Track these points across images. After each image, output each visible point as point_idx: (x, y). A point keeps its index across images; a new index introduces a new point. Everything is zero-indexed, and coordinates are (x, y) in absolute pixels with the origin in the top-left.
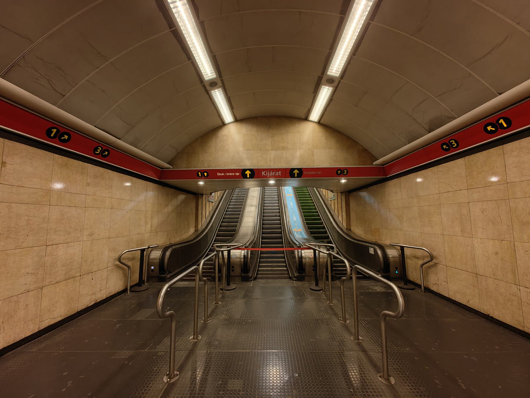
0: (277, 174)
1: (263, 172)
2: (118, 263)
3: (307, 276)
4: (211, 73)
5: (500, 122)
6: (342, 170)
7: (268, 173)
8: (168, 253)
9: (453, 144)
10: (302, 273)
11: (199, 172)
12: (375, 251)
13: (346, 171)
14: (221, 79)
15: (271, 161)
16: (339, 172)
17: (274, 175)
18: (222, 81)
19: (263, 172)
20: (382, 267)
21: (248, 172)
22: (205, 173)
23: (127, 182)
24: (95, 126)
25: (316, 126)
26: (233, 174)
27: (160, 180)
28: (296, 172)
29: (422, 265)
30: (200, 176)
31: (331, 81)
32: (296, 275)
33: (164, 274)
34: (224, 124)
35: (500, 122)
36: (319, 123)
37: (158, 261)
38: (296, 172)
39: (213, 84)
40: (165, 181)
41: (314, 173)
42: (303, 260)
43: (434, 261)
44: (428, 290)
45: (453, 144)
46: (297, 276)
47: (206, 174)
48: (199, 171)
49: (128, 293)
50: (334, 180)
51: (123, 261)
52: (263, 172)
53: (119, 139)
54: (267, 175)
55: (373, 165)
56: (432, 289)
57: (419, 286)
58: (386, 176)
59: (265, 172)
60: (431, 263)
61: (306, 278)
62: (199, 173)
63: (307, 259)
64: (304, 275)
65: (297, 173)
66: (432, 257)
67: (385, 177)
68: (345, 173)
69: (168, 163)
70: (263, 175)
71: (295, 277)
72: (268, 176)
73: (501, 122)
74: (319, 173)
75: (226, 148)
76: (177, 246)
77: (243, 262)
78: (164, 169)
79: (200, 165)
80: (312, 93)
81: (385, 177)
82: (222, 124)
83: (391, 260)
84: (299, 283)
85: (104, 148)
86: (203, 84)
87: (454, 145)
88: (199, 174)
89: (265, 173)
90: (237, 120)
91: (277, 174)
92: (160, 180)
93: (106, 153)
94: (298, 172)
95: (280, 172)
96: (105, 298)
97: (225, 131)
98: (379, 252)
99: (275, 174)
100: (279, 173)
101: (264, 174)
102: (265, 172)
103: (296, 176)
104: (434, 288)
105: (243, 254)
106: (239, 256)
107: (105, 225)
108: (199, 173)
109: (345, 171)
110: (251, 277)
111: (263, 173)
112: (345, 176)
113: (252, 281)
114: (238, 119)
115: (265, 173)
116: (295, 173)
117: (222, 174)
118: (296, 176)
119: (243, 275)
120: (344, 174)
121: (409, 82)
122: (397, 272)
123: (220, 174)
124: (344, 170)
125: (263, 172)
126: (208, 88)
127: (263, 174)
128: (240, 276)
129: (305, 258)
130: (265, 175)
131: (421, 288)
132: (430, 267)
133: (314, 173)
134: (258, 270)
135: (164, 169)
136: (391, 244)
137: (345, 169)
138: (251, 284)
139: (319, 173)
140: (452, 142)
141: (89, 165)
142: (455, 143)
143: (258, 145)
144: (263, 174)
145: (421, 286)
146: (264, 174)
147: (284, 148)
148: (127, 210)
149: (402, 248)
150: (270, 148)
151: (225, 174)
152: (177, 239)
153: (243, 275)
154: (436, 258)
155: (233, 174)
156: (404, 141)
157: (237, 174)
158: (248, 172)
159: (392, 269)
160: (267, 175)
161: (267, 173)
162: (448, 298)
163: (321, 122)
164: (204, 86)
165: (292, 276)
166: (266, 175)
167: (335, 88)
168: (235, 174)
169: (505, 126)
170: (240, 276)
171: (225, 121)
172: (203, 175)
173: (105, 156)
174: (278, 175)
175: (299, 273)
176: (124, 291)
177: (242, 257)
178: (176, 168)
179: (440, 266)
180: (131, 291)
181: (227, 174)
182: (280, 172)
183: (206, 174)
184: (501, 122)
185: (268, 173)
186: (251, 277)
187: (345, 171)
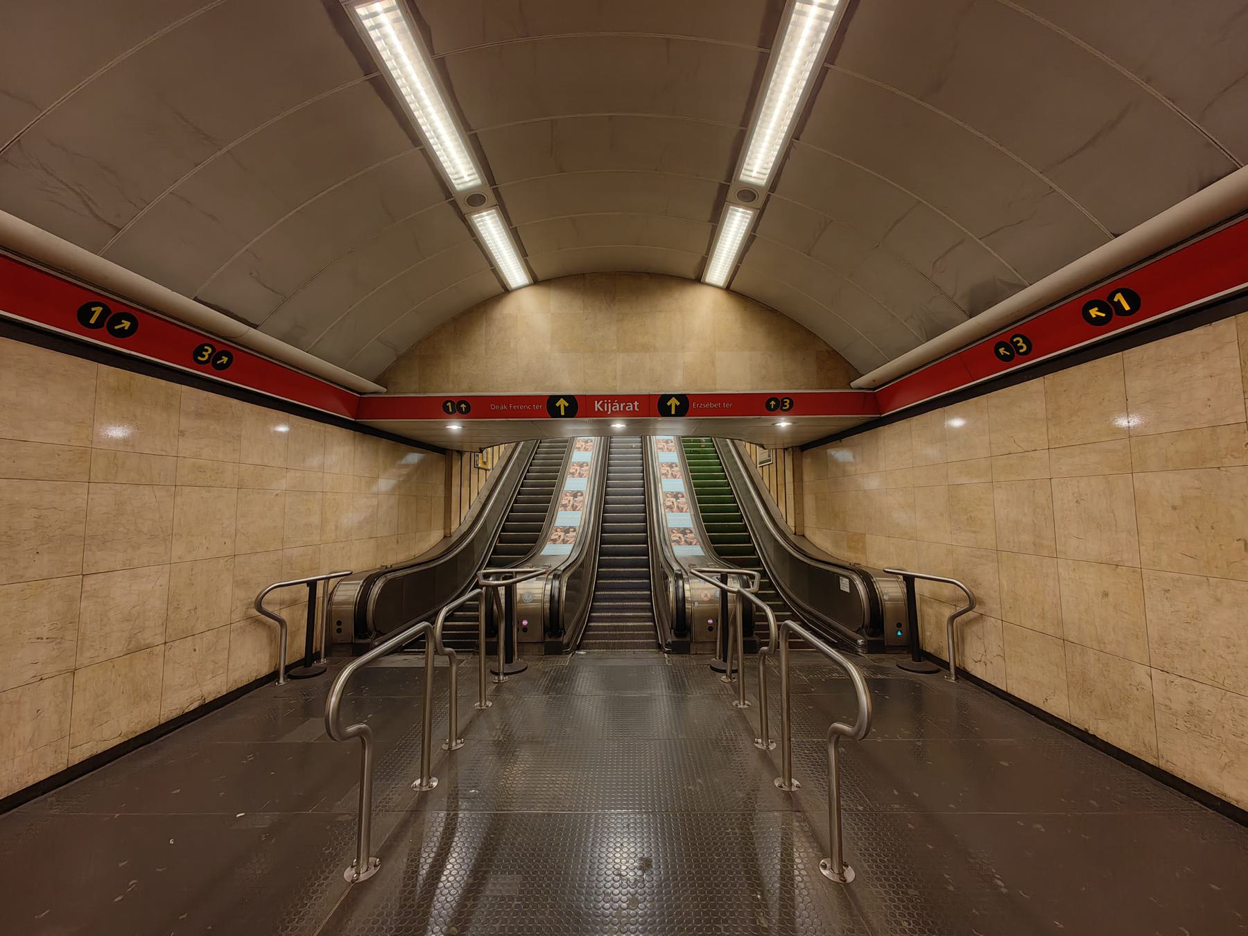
0: (629, 408)
1: (598, 403)
2: (255, 612)
3: (696, 642)
4: (469, 175)
5: (1116, 300)
6: (780, 399)
7: (610, 404)
8: (376, 590)
9: (1019, 345)
10: (685, 636)
11: (447, 402)
12: (852, 585)
14: (493, 189)
18: (496, 192)
19: (596, 402)
20: (867, 621)
21: (562, 403)
23: (277, 423)
24: (196, 299)
25: (721, 297)
26: (528, 407)
28: (673, 402)
29: (953, 618)
30: (451, 411)
31: (748, 195)
32: (670, 640)
33: (366, 637)
34: (506, 290)
35: (1116, 300)
36: (728, 288)
37: (351, 607)
38: (673, 402)
39: (476, 200)
42: (688, 606)
43: (978, 609)
44: (963, 674)
45: (1019, 345)
46: (673, 641)
48: (448, 399)
49: (281, 681)
50: (764, 421)
51: (269, 609)
52: (596, 402)
53: (255, 326)
54: (606, 410)
55: (852, 388)
56: (973, 673)
57: (946, 665)
58: (881, 414)
59: (601, 402)
60: (971, 614)
61: (693, 648)
63: (696, 604)
64: (688, 639)
65: (676, 405)
66: (972, 602)
68: (786, 406)
69: (377, 381)
70: (596, 410)
71: (668, 645)
72: (609, 413)
73: (1119, 300)
75: (512, 346)
76: (399, 574)
77: (548, 611)
78: (365, 393)
79: (451, 386)
80: (709, 222)
82: (503, 291)
83: (888, 605)
84: (675, 657)
85: (219, 348)
86: (450, 200)
87: (1022, 347)
88: (448, 406)
89: (602, 406)
90: (536, 281)
91: (630, 407)
93: (225, 359)
94: (678, 404)
95: (636, 403)
96: (225, 693)
97: (509, 307)
98: (861, 588)
99: (624, 407)
100: (634, 406)
101: (600, 408)
102: (601, 402)
103: (673, 412)
104: (978, 671)
105: (549, 593)
106: (539, 596)
107: (224, 526)
108: (449, 404)
109: (786, 402)
110: (568, 645)
111: (597, 406)
112: (786, 412)
113: (568, 653)
114: (540, 278)
117: (502, 408)
118: (673, 412)
119: (548, 640)
121: (920, 202)
122: (899, 633)
125: (598, 403)
126: (465, 208)
127: (598, 408)
128: (542, 643)
129: (692, 602)
131: (949, 669)
132: (969, 623)
135: (365, 393)
136: (887, 570)
138: (565, 661)
140: (1018, 342)
141: (185, 388)
142: (1023, 343)
143: (586, 339)
144: (598, 408)
145: (949, 664)
146: (600, 408)
147: (646, 348)
148: (278, 492)
149: (909, 580)
150: (615, 348)
153: (548, 640)
154: (982, 603)
155: (528, 407)
156: (917, 335)
158: (562, 403)
159: (889, 625)
160: (606, 410)
161: (606, 405)
162: (1006, 693)
163: (731, 288)
164: (454, 204)
165: (662, 642)
166: (604, 409)
167: (759, 211)
169: (1127, 308)
170: (542, 643)
173: (223, 366)
174: (631, 409)
175: (677, 635)
176: (272, 677)
177: (547, 598)
178: (395, 393)
179: (990, 622)
182: (636, 403)
184: (1119, 300)
185: (610, 404)
186: (568, 645)
187: (786, 402)
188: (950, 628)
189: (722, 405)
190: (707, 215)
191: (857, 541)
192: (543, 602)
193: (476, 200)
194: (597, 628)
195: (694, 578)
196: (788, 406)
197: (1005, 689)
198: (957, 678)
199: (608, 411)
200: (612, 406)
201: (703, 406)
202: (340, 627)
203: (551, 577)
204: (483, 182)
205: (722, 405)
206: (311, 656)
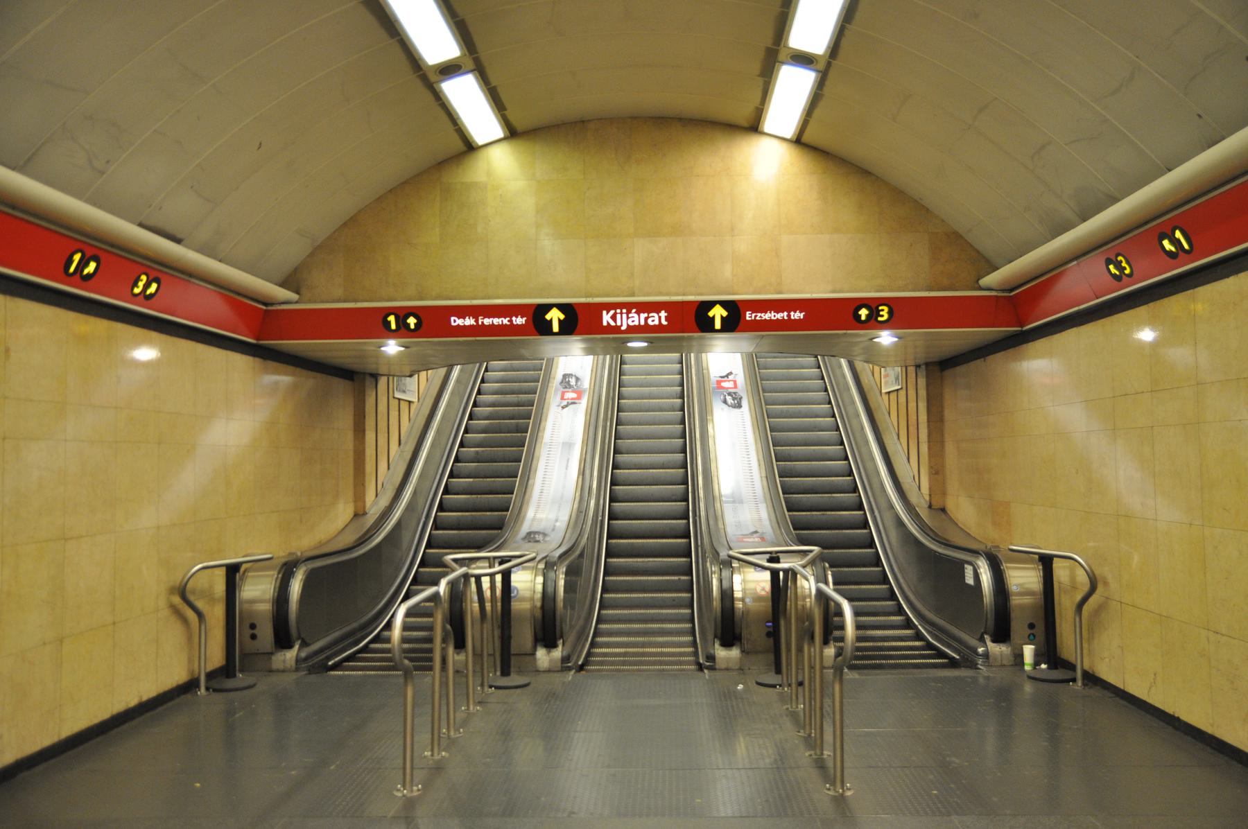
0: (653, 321)
2: (177, 600)
6: (874, 307)
7: (624, 316)
8: (296, 587)
12: (977, 576)
13: (886, 308)
15: (632, 274)
16: (864, 313)
17: (642, 323)
19: (604, 312)
21: (555, 316)
22: (408, 318)
23: (150, 343)
24: (141, 225)
26: (506, 321)
27: (261, 342)
31: (803, 59)
34: (470, 147)
36: (798, 141)
39: (449, 69)
40: (281, 344)
41: (779, 316)
44: (1091, 679)
47: (412, 321)
48: (390, 311)
53: (178, 241)
55: (981, 289)
57: (1072, 667)
59: (612, 312)
62: (392, 319)
67: (1020, 329)
68: (882, 316)
69: (283, 284)
74: (797, 315)
78: (272, 304)
81: (1020, 329)
82: (465, 149)
88: (390, 322)
89: (614, 318)
90: (512, 133)
91: (654, 319)
92: (261, 342)
94: (725, 314)
95: (663, 314)
99: (646, 319)
100: (660, 318)
102: (612, 312)
108: (392, 319)
109: (883, 310)
111: (606, 318)
114: (519, 125)
115: (614, 318)
116: (714, 316)
120: (880, 319)
123: (460, 322)
124: (881, 308)
126: (433, 78)
130: (612, 323)
133: (779, 316)
134: (593, 645)
135: (272, 304)
137: (884, 301)
139: (797, 315)
147: (678, 230)
149: (1046, 562)
151: (477, 321)
152: (305, 543)
154: (1106, 584)
155: (506, 321)
157: (519, 321)
158: (555, 316)
160: (619, 324)
161: (618, 316)
166: (615, 321)
168: (511, 321)
171: (474, 141)
172: (402, 322)
176: (189, 687)
177: (539, 596)
178: (310, 301)
180: (207, 689)
181: (482, 322)
183: (412, 321)
187: (883, 310)
188: (1077, 619)
189: (789, 316)
190: (756, 67)
191: (998, 512)
192: (532, 599)
193: (449, 69)
194: (608, 645)
195: (746, 567)
196: (886, 317)
197: (1122, 688)
198: (1084, 685)
199: (622, 325)
200: (628, 318)
201: (761, 317)
202: (252, 632)
203: (541, 566)
204: (462, 54)
205: (789, 316)
206: (227, 670)
